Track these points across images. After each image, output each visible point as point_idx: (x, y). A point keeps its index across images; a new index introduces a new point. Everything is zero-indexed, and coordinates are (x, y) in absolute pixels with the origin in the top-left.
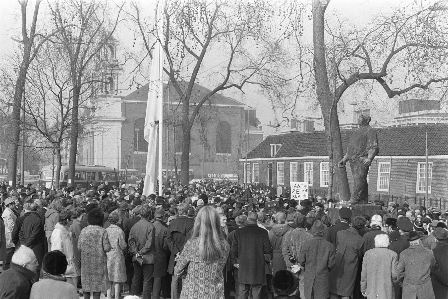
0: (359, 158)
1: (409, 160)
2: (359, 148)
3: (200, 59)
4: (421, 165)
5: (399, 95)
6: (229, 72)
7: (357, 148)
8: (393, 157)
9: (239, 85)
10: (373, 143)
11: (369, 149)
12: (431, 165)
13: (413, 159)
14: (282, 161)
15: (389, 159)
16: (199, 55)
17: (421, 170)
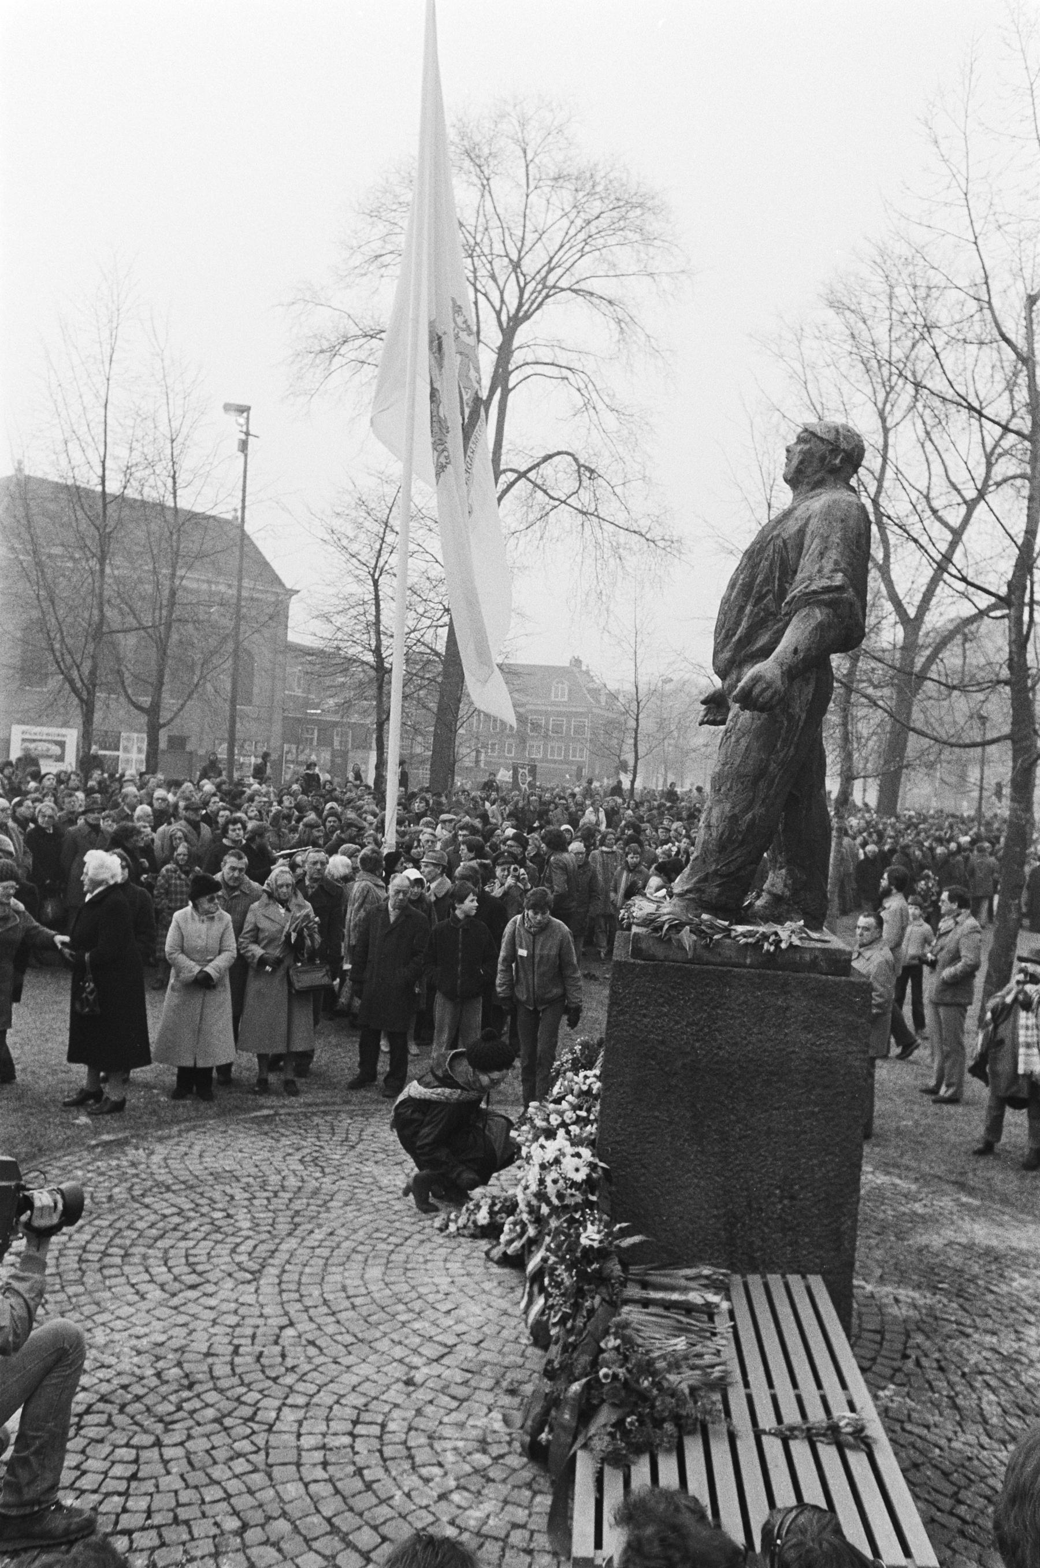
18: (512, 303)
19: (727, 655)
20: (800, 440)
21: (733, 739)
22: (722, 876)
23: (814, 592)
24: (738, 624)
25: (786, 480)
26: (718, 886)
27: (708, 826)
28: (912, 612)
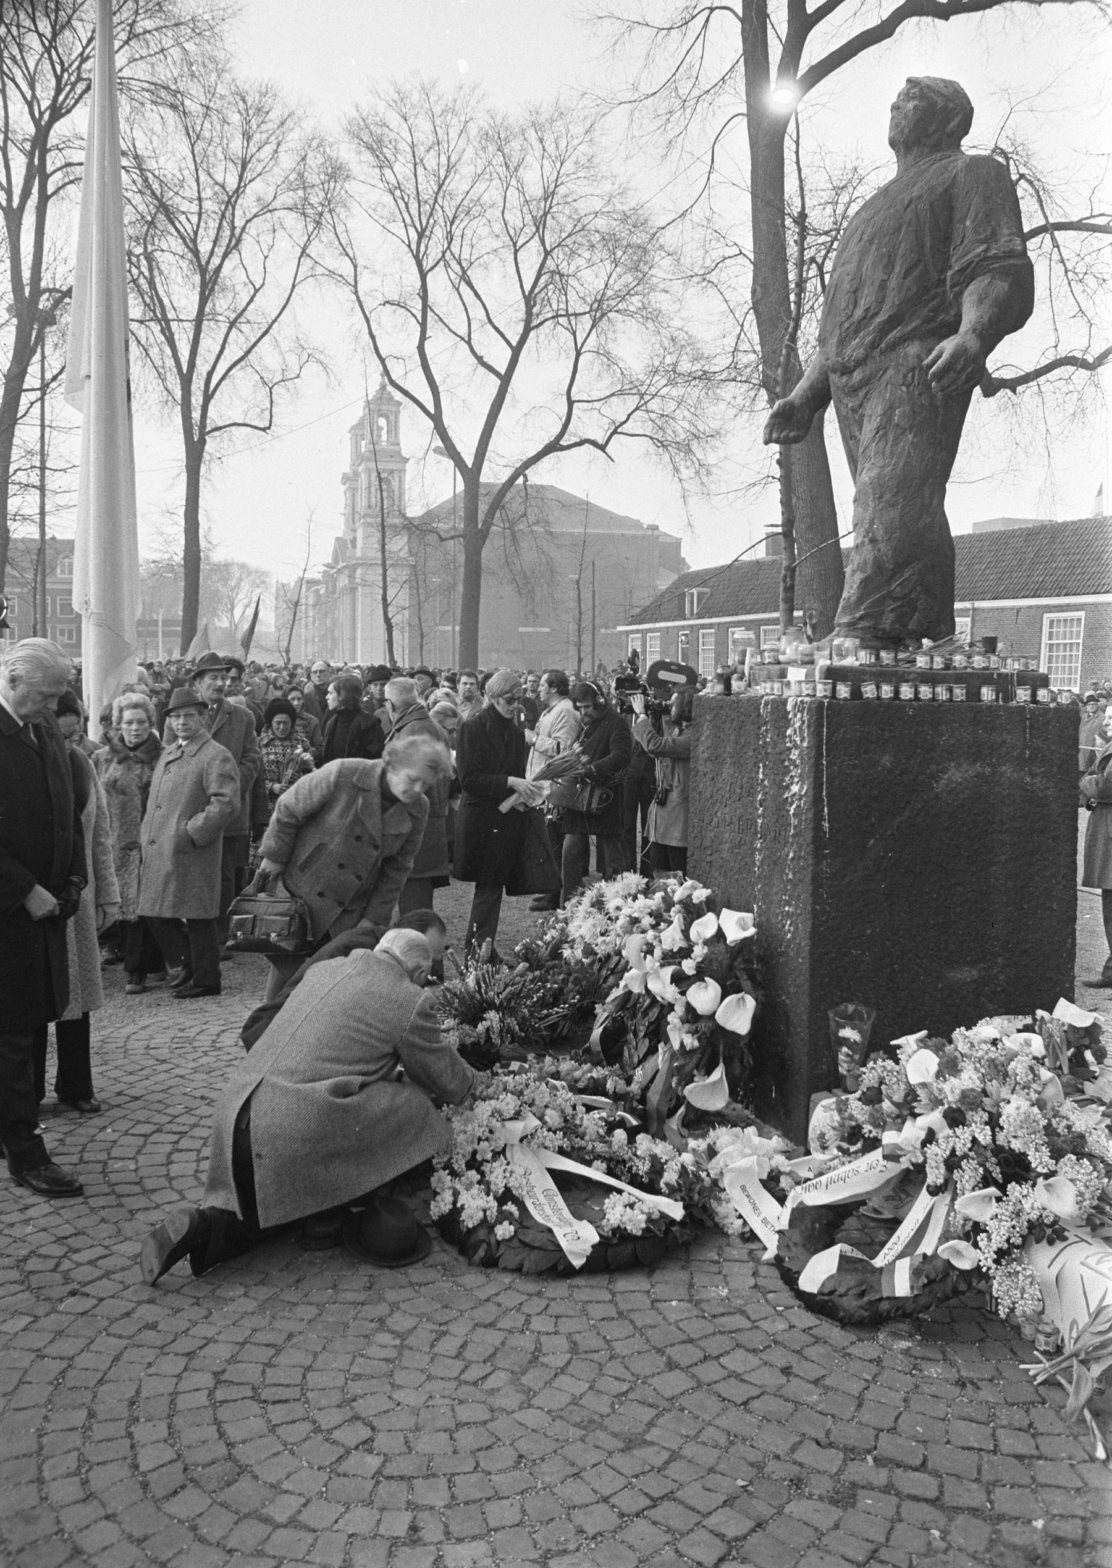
0: (893, 346)
1: (1019, 610)
2: (893, 283)
3: (505, 380)
4: (1052, 622)
5: (1014, 391)
6: (571, 403)
7: (883, 286)
8: (979, 604)
9: (601, 441)
10: (993, 237)
11: (968, 275)
12: (1079, 620)
13: (1030, 607)
14: (711, 626)
15: (967, 610)
16: (502, 371)
17: (1051, 633)
18: (45, 104)
19: (867, 336)
20: (905, 96)
21: (891, 437)
22: (895, 599)
23: (996, 257)
24: (881, 302)
25: (893, 144)
26: (892, 610)
27: (873, 541)
28: (469, 462)
